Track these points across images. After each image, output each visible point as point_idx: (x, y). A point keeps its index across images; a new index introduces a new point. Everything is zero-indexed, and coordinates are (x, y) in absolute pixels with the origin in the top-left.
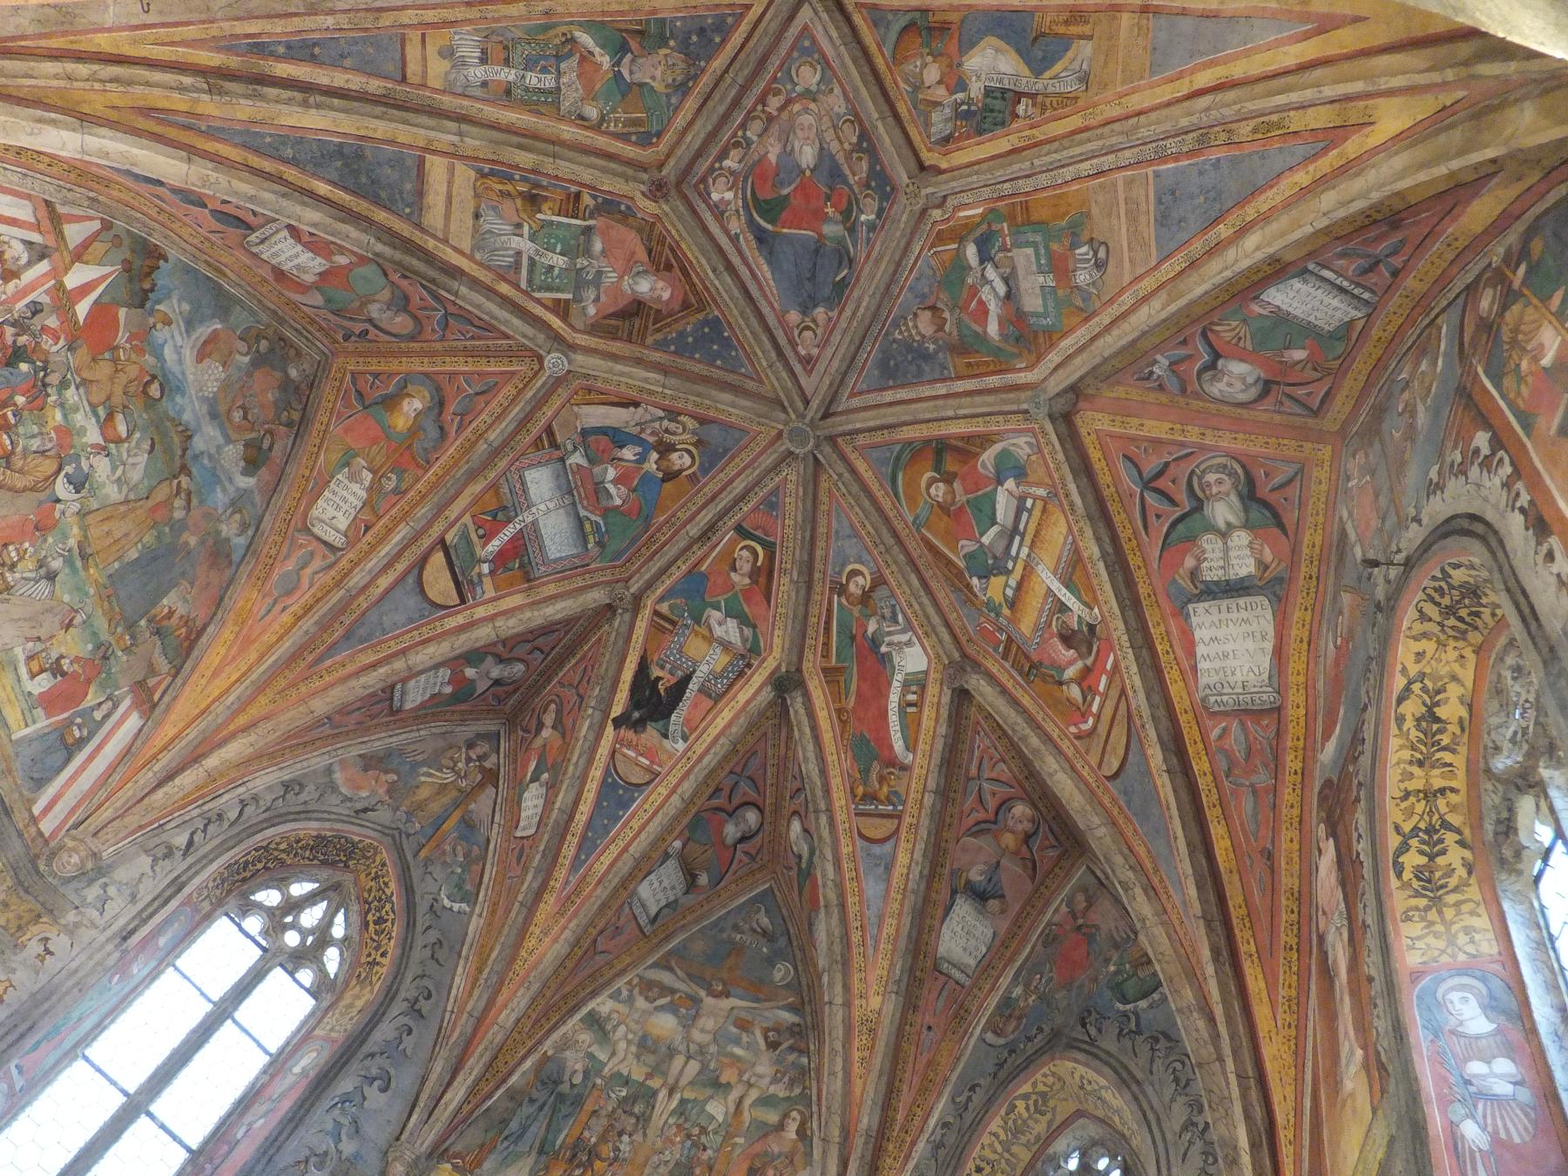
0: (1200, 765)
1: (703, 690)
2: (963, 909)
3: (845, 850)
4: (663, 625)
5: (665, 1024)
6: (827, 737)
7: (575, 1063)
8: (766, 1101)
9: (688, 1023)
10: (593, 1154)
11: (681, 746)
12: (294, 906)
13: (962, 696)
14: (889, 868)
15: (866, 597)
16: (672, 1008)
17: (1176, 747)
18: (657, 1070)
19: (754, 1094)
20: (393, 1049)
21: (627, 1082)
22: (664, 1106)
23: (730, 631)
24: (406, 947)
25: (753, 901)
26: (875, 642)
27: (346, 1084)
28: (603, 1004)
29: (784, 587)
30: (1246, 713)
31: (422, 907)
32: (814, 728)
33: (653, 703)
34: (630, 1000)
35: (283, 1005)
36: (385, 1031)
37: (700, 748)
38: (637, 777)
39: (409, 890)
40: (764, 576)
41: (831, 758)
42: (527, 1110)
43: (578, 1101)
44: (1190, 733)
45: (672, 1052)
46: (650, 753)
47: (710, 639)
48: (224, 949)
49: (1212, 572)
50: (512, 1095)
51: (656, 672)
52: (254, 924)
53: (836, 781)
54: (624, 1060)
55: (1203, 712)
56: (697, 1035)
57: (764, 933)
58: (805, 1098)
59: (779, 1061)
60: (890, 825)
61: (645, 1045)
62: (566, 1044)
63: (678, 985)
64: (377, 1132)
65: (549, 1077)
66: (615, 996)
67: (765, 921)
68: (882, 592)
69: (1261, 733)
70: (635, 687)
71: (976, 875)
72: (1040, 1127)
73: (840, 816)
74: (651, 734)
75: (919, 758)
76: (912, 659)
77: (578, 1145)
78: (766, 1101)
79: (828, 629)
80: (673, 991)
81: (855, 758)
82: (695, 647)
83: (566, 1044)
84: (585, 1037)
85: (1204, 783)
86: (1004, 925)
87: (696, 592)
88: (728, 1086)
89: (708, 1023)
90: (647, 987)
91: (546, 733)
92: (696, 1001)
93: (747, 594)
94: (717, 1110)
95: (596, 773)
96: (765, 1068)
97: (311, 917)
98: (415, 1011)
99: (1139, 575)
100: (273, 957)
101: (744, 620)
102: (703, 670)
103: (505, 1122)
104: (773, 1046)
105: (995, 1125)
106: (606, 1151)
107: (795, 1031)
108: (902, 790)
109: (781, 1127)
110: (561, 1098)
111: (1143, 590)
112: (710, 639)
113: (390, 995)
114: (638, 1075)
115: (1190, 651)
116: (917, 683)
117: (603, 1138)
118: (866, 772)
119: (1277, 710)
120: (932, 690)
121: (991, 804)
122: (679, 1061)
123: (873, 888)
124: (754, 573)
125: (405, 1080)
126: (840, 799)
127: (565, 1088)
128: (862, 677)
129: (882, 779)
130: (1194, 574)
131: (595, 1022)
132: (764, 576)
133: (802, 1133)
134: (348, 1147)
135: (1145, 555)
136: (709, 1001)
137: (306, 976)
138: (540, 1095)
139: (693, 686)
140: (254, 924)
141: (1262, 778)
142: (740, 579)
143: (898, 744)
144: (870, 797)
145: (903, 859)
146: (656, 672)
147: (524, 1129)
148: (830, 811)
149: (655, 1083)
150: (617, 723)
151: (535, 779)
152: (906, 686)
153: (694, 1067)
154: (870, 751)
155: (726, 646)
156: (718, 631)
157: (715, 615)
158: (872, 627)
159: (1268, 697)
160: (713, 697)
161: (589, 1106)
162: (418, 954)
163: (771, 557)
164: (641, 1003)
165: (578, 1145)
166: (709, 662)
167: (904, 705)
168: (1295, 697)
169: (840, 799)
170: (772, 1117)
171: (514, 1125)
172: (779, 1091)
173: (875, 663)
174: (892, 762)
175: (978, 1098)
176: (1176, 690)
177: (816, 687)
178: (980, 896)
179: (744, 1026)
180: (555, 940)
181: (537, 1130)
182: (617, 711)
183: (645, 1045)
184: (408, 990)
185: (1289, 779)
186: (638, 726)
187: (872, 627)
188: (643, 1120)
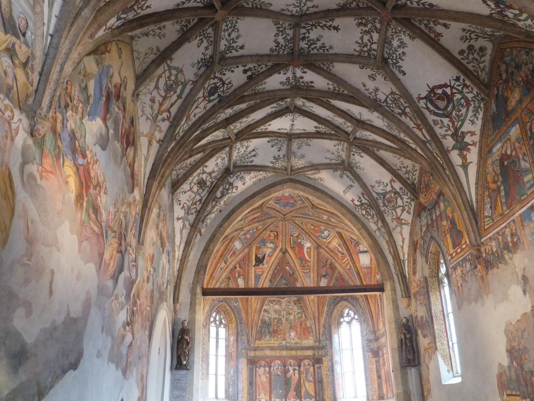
0: (361, 275)
1: (268, 256)
2: (323, 279)
3: (301, 275)
4: (258, 248)
5: (277, 307)
6: (293, 258)
7: (267, 319)
8: (298, 313)
9: (281, 305)
10: (277, 331)
11: (267, 266)
12: (215, 318)
13: (318, 254)
14: (310, 277)
15: (297, 237)
16: (277, 304)
17: (358, 274)
18: (280, 315)
19: (296, 313)
20: (241, 330)
21: (276, 318)
22: (284, 320)
23: (272, 245)
24: (235, 315)
25: (281, 278)
26: (300, 243)
27: (239, 339)
28: (265, 307)
29: (280, 237)
30: (367, 268)
31: (233, 308)
32: (291, 257)
33: (259, 261)
34: (269, 305)
35: (222, 331)
36: (239, 328)
37: (270, 265)
38: (260, 273)
39: (230, 307)
40: (276, 237)
41: (295, 261)
42: (264, 329)
43: (271, 324)
44: (360, 271)
45: (280, 311)
46: (261, 269)
47: (268, 248)
48: (213, 329)
49: (361, 249)
50: (260, 327)
51: (259, 256)
52: (213, 324)
53: (297, 264)
54: (274, 315)
55: (361, 268)
56: (283, 307)
57: (285, 284)
58: (304, 311)
59: (297, 306)
60: (309, 270)
61: (276, 311)
62: (263, 316)
63: (276, 299)
64: (246, 341)
65: (264, 322)
66: (266, 305)
67: (284, 281)
68: (300, 236)
69: (369, 270)
70: (256, 259)
71: (324, 274)
72: (341, 309)
73: (299, 270)
74: (261, 266)
75: (312, 259)
76: (308, 245)
77: (274, 331)
78: (298, 313)
79: (290, 241)
80: (275, 301)
81: (300, 261)
82: (265, 250)
83: (263, 316)
84: (266, 314)
85: (362, 277)
86: (329, 278)
87: (264, 242)
88: (291, 314)
89: (283, 304)
90: (271, 301)
91: (238, 269)
92: (280, 301)
93: (274, 239)
94: (292, 317)
95: (253, 275)
96: (296, 308)
97: (218, 318)
98: (241, 323)
99: (351, 250)
100: (217, 327)
101: (273, 243)
102: (267, 253)
103: (261, 332)
104: (295, 304)
105: (335, 311)
106: (279, 329)
107: (298, 300)
108: (309, 264)
109: (302, 316)
110: (268, 325)
111: (352, 252)
112: (268, 248)
113: (237, 323)
114: (277, 317)
115: (359, 260)
116: (310, 248)
117: (277, 328)
118: (302, 263)
119: (371, 267)
120: (312, 249)
121: (324, 262)
122: (282, 312)
123: (308, 280)
124: (275, 236)
125: (244, 333)
126: (298, 267)
127: (267, 323)
128: (298, 248)
129: (305, 263)
130: (359, 250)
131: (266, 311)
132: (276, 237)
133: (305, 316)
134: (244, 345)
135: (352, 247)
136: (282, 300)
137: (222, 326)
138: (264, 326)
139: (266, 256)
140: (213, 324)
141: (369, 276)
142: (272, 238)
143: (307, 258)
144: (304, 266)
145: (312, 275)
146: (259, 256)
147: (265, 331)
148: (297, 270)
149: (280, 317)
150: (254, 266)
151: (239, 277)
152: (307, 249)
153: (285, 312)
154: (302, 259)
155: (271, 248)
156: (269, 246)
157: (268, 244)
158: (299, 241)
159: (370, 266)
160: (270, 256)
161: (272, 324)
162: (237, 315)
163: (277, 233)
164: (271, 305)
165: (274, 331)
166: (268, 251)
167: (307, 252)
168: (373, 266)
169: (298, 267)
170: (300, 316)
171: (263, 331)
172: (299, 311)
173: (301, 246)
174: (307, 260)
175: (332, 307)
176: (357, 265)
177: (290, 250)
178: (325, 276)
179: (289, 302)
180: (257, 304)
181: (267, 330)
182: (253, 264)
183: (276, 311)
184: (238, 321)
185: (373, 276)
186: (258, 265)
187: (299, 241)
188: (281, 323)
